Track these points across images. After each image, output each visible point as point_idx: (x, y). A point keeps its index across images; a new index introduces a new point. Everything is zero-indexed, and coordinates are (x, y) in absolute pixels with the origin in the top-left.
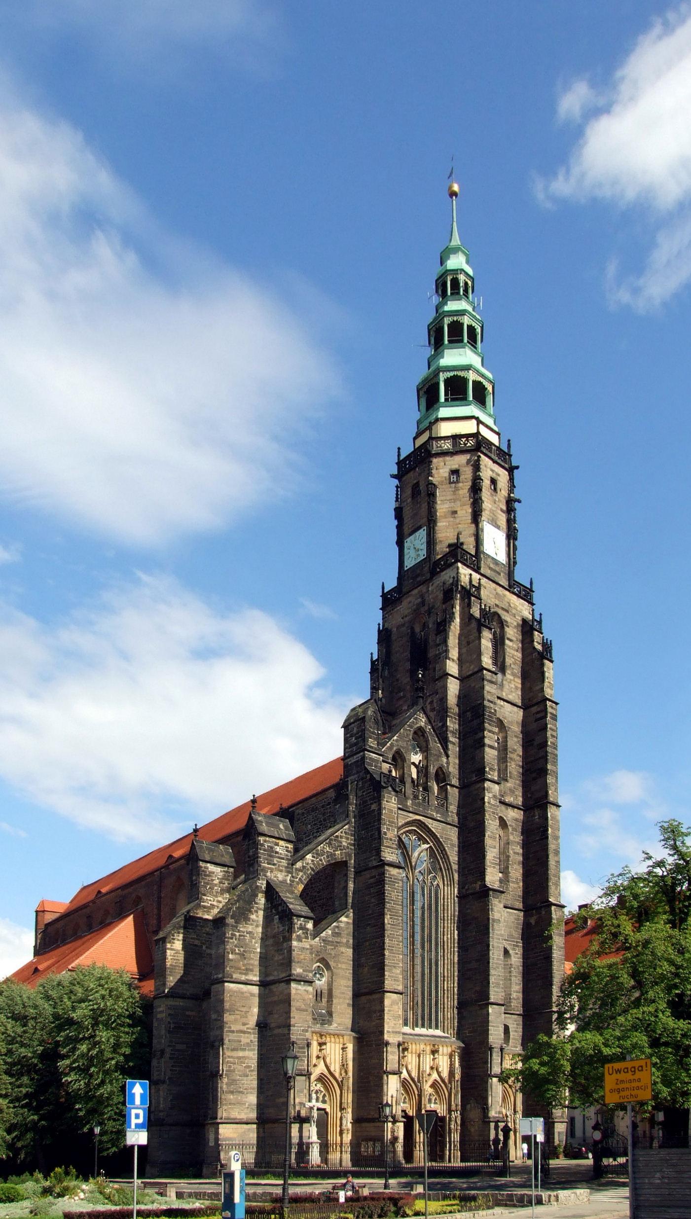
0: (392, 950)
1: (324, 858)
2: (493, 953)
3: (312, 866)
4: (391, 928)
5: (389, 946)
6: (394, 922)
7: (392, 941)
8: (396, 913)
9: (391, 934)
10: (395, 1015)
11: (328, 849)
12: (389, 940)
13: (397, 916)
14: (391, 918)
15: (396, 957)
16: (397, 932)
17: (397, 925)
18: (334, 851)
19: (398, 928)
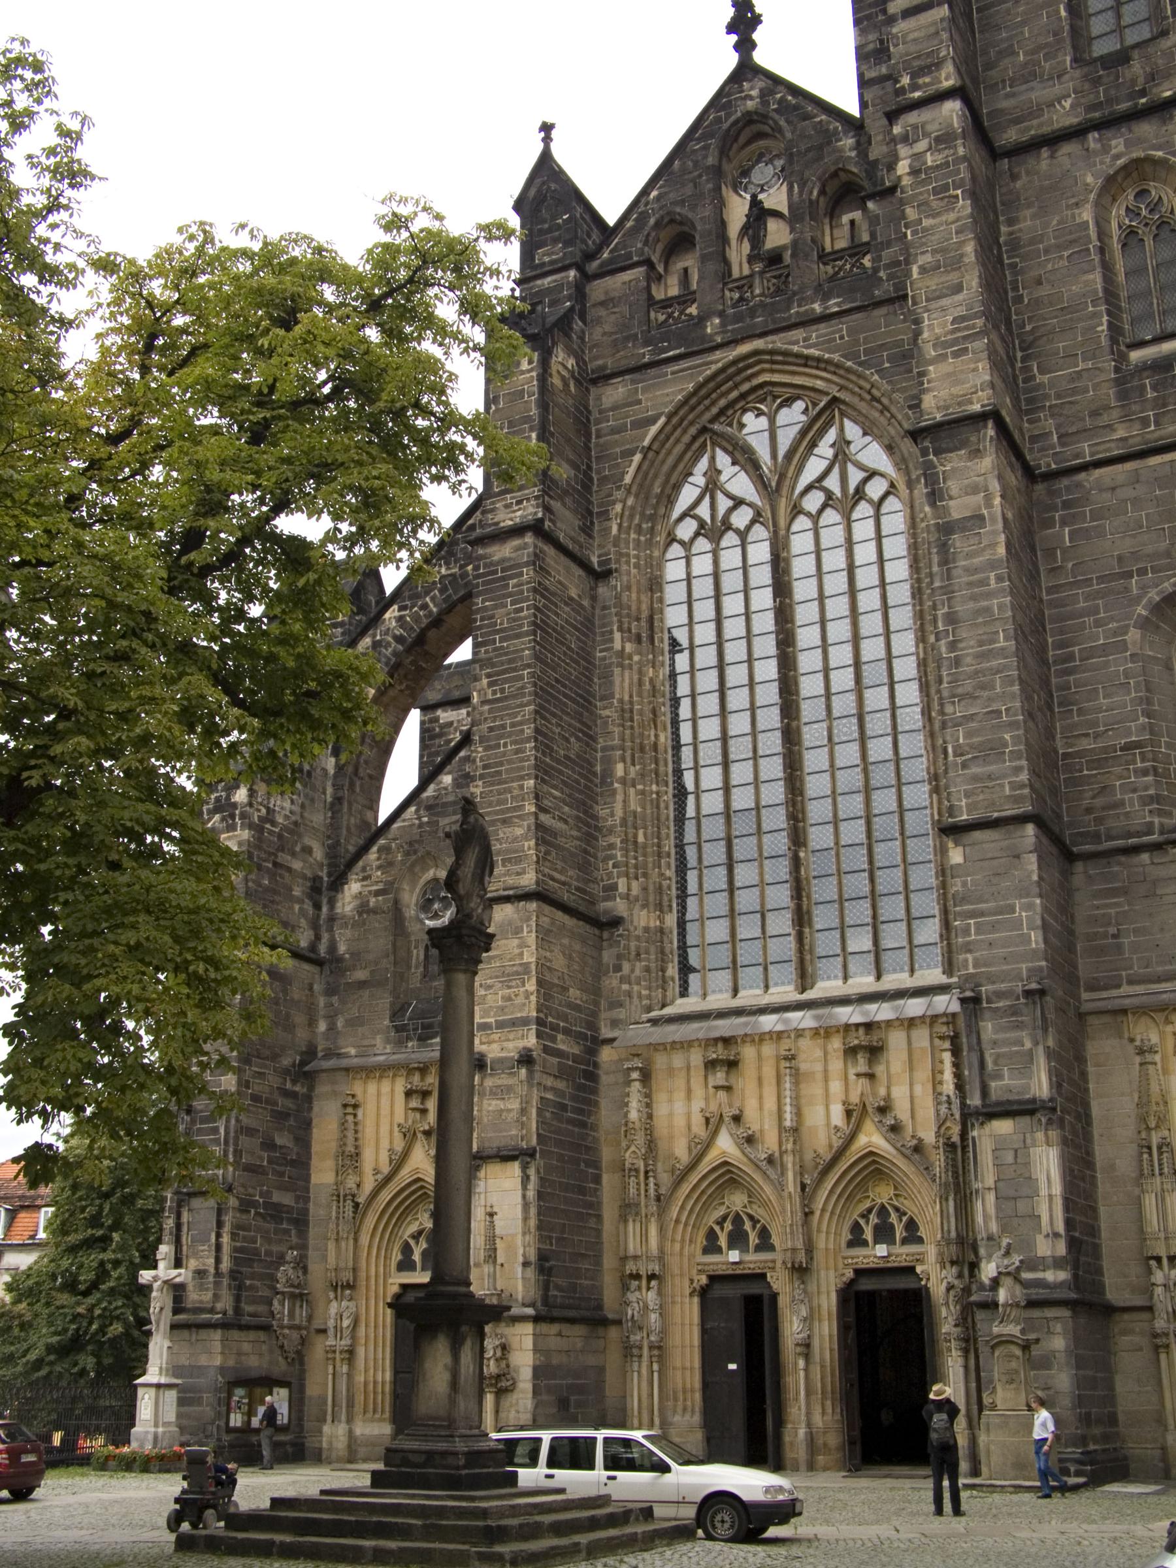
0: (499, 773)
1: (433, 599)
2: (953, 646)
3: (399, 632)
4: (490, 711)
5: (485, 767)
6: (502, 691)
7: (498, 746)
8: (510, 661)
9: (491, 729)
10: (509, 970)
11: (443, 571)
12: (486, 749)
13: (515, 670)
14: (490, 684)
15: (506, 791)
16: (515, 715)
17: (514, 697)
18: (461, 567)
19: (518, 702)
